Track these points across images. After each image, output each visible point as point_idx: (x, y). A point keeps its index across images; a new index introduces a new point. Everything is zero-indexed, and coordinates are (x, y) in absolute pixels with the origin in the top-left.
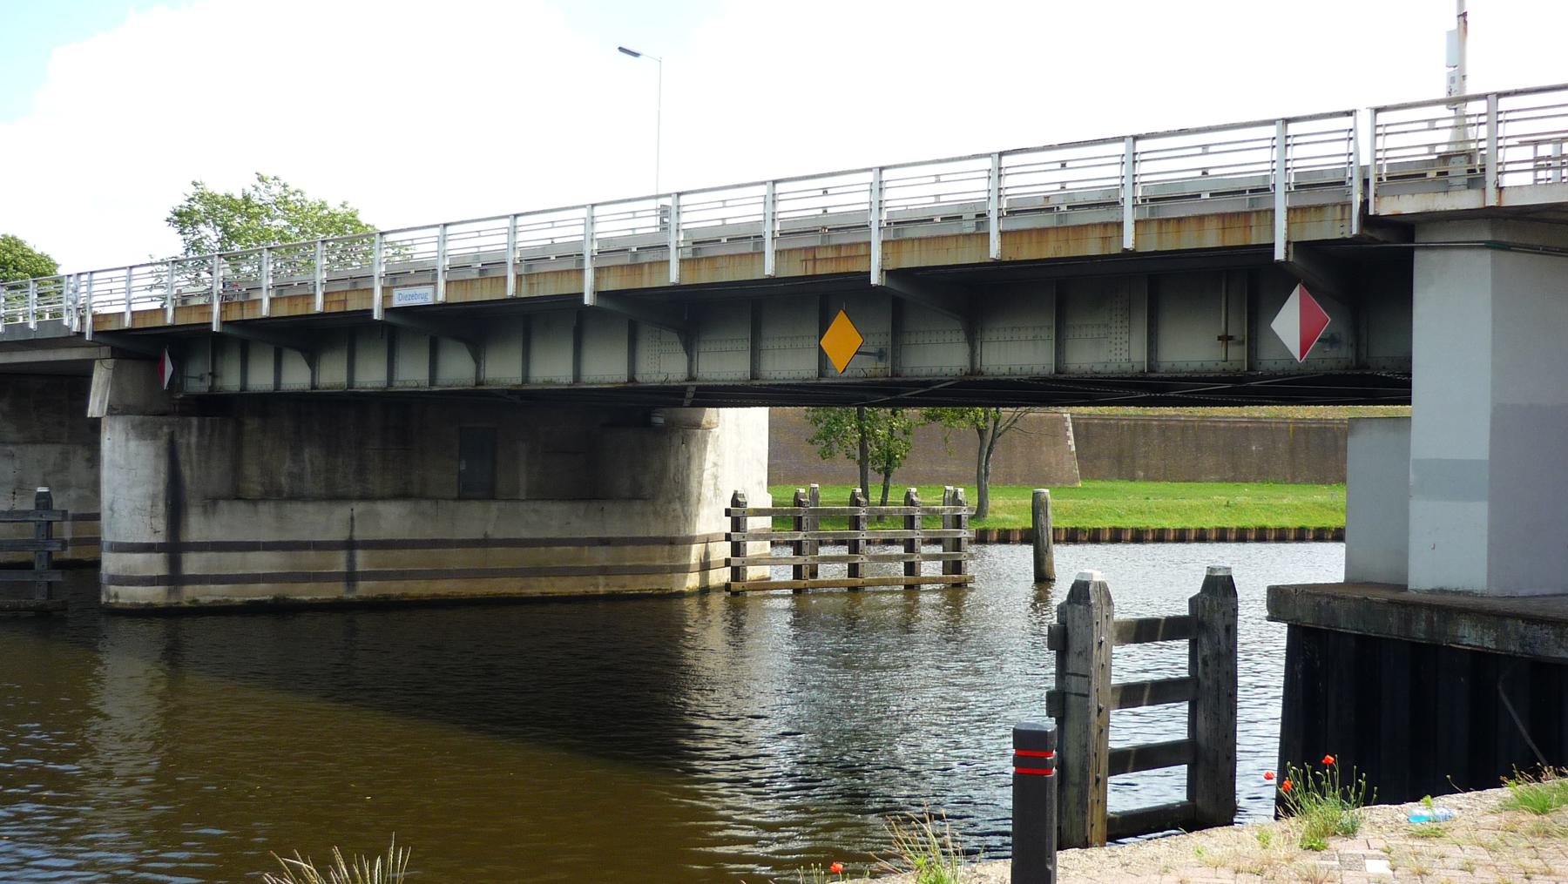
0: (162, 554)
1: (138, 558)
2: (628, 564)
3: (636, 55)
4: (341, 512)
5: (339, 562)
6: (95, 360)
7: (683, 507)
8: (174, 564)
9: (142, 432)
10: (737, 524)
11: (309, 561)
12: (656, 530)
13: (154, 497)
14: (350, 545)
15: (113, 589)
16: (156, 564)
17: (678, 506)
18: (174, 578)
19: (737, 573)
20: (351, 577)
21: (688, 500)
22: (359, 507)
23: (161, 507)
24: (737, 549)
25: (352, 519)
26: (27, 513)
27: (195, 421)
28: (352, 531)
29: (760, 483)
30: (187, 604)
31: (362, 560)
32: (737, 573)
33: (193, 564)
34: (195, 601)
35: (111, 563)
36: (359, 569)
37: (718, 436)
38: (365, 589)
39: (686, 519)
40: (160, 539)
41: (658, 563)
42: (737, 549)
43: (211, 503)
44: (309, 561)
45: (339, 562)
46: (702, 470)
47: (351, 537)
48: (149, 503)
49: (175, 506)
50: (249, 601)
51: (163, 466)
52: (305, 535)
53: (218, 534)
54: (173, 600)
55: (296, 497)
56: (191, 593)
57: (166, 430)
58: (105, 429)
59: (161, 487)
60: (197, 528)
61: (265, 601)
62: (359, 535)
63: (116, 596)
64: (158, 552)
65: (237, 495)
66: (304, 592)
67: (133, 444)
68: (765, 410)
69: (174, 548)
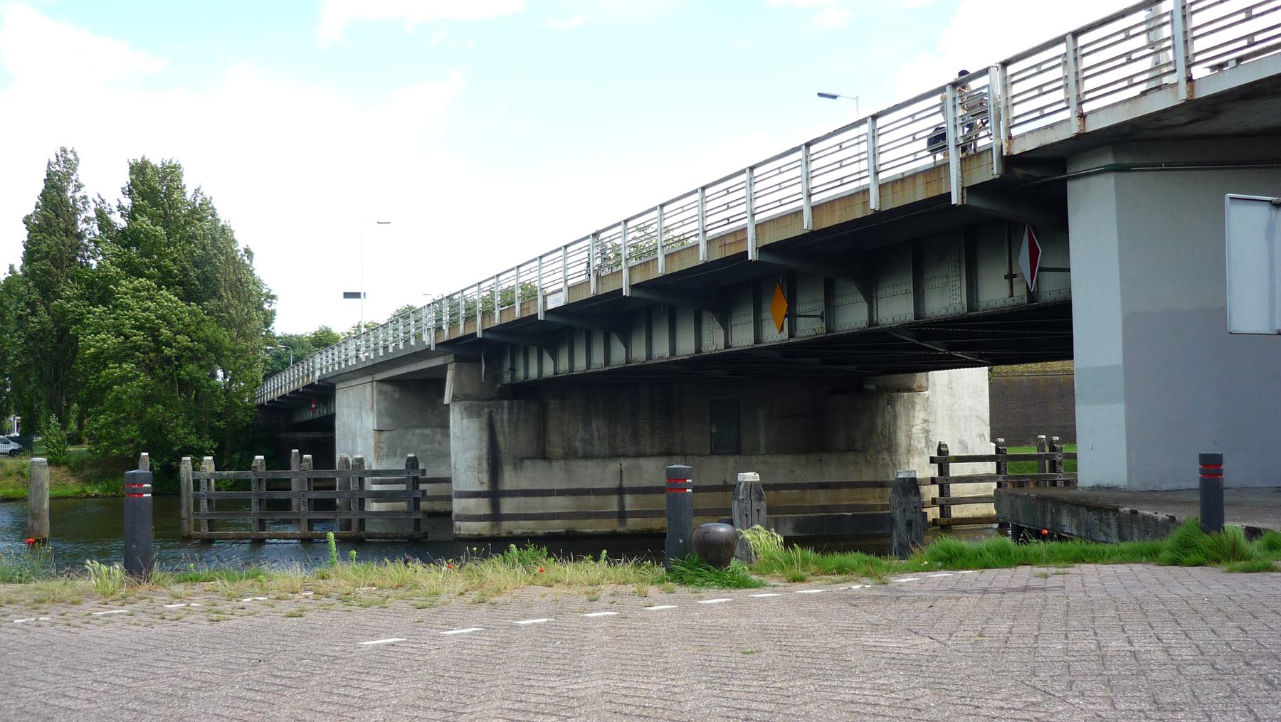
0: (486, 499)
1: (472, 501)
2: (844, 503)
3: (834, 97)
4: (613, 466)
5: (612, 504)
6: (448, 364)
7: (891, 457)
8: (495, 506)
9: (471, 413)
10: (943, 470)
11: (591, 503)
12: (868, 476)
13: (480, 459)
14: (620, 491)
15: (457, 524)
16: (482, 506)
17: (886, 456)
18: (496, 516)
19: (945, 511)
20: (622, 515)
21: (896, 451)
22: (625, 463)
23: (485, 465)
24: (944, 491)
25: (621, 471)
26: (399, 472)
27: (506, 403)
28: (621, 480)
29: (982, 436)
30: (505, 535)
31: (630, 502)
32: (945, 511)
33: (508, 506)
34: (510, 533)
35: (458, 506)
36: (627, 509)
37: (928, 398)
38: (633, 524)
39: (895, 466)
40: (485, 488)
41: (871, 502)
42: (944, 491)
43: (519, 461)
44: (591, 503)
45: (612, 504)
46: (910, 426)
47: (621, 485)
48: (476, 462)
49: (494, 468)
50: (548, 533)
51: (485, 437)
52: (587, 484)
53: (525, 485)
54: (495, 532)
55: (587, 456)
56: (507, 527)
57: (486, 410)
58: (453, 410)
59: (485, 451)
60: (510, 480)
61: (559, 533)
62: (627, 483)
63: (460, 529)
64: (484, 497)
65: (543, 455)
66: (588, 527)
67: (465, 421)
68: (984, 371)
69: (494, 494)
